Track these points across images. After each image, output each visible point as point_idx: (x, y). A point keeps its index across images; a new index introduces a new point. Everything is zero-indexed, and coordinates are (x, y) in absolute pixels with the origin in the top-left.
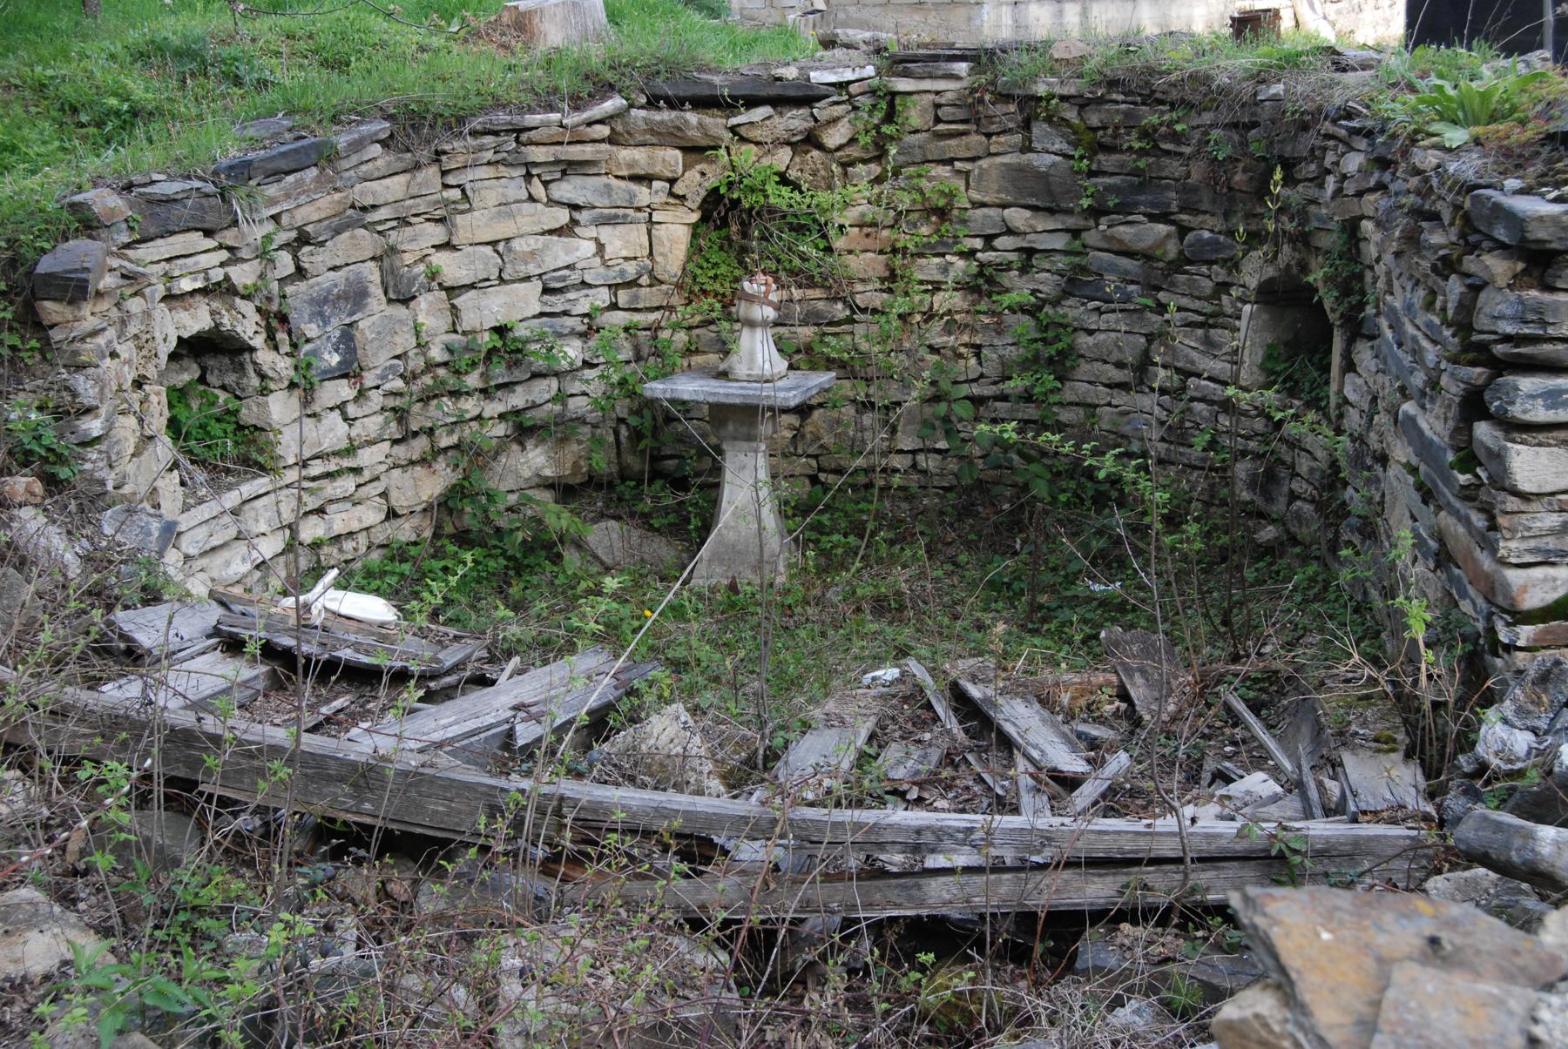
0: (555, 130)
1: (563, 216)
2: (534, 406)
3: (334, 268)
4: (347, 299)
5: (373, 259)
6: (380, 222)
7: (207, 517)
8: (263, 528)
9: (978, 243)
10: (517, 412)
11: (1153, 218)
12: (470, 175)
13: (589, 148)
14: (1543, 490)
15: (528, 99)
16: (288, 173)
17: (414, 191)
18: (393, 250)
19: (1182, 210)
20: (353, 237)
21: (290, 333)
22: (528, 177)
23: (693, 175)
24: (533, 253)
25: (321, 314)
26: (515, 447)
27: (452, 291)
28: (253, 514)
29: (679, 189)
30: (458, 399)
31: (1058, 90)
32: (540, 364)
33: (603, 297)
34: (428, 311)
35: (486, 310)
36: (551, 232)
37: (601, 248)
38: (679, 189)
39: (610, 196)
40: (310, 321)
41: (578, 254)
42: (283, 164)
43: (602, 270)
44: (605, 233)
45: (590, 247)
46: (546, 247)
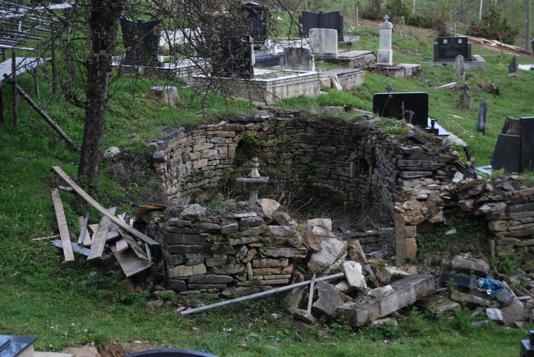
1: (212, 145)
2: (205, 184)
9: (294, 150)
10: (201, 186)
11: (332, 146)
13: (219, 132)
15: (207, 122)
19: (338, 144)
22: (206, 138)
23: (237, 137)
27: (193, 161)
29: (235, 139)
31: (313, 121)
32: (206, 176)
33: (218, 162)
35: (198, 164)
38: (235, 139)
44: (220, 149)
45: (216, 151)
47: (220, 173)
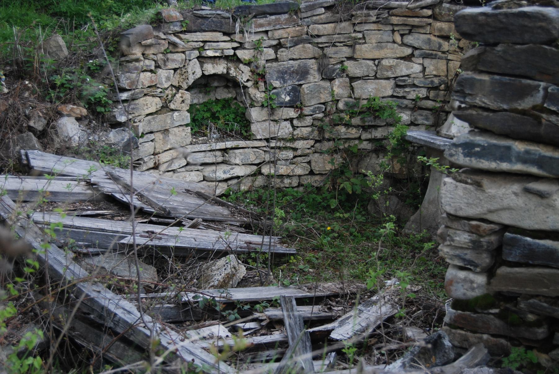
0: (404, 10)
3: (293, 59)
4: (297, 74)
5: (314, 58)
6: (322, 43)
7: (203, 149)
8: (237, 161)
12: (367, 27)
14: (461, 213)
16: (271, 14)
17: (338, 31)
18: (325, 56)
20: (304, 47)
21: (265, 83)
22: (393, 31)
24: (391, 67)
25: (283, 78)
26: (374, 155)
27: (353, 79)
28: (234, 155)
30: (348, 128)
34: (339, 87)
35: (368, 90)
36: (401, 58)
37: (424, 69)
39: (430, 44)
40: (277, 80)
41: (412, 70)
42: (268, 10)
43: (422, 80)
46: (397, 64)
47: (427, 119)
